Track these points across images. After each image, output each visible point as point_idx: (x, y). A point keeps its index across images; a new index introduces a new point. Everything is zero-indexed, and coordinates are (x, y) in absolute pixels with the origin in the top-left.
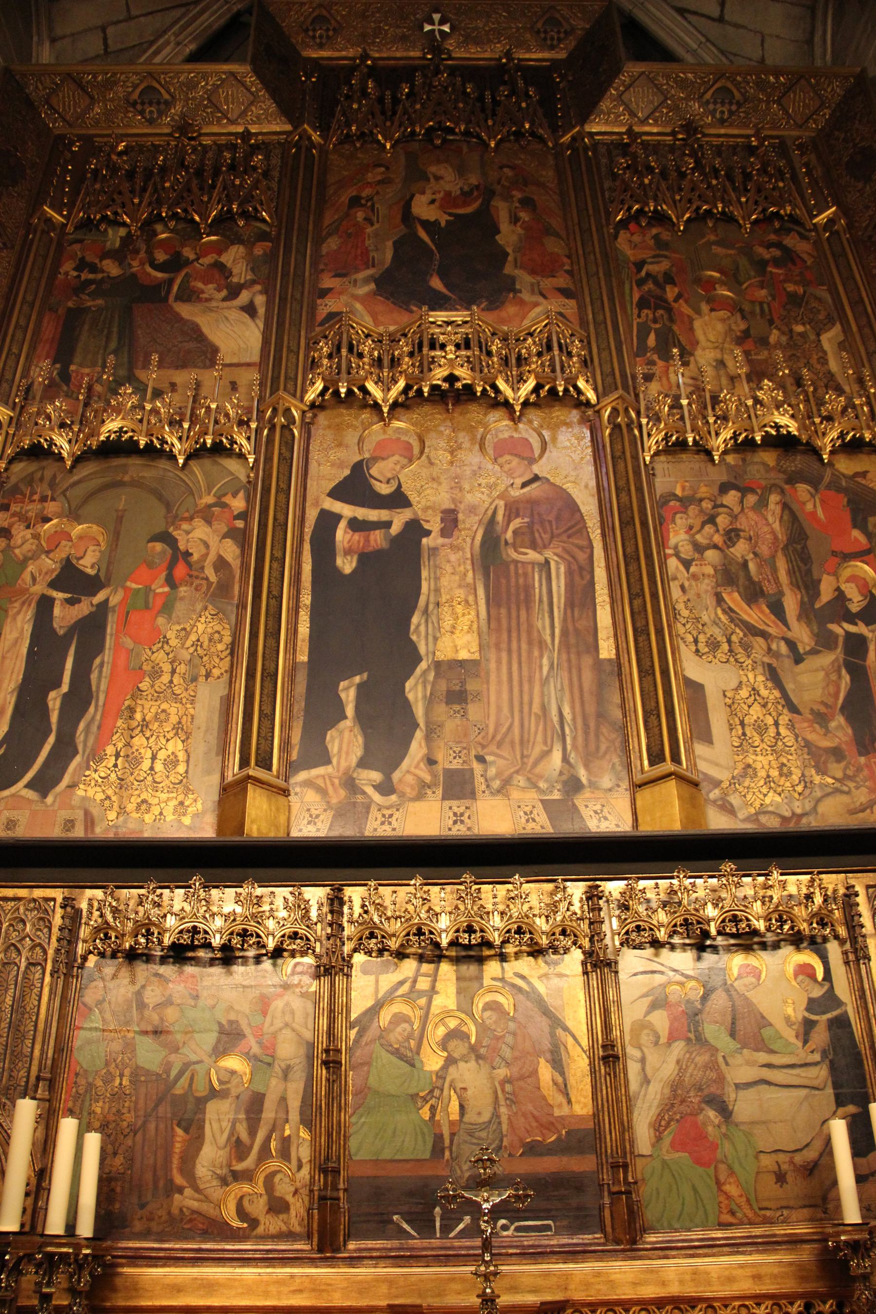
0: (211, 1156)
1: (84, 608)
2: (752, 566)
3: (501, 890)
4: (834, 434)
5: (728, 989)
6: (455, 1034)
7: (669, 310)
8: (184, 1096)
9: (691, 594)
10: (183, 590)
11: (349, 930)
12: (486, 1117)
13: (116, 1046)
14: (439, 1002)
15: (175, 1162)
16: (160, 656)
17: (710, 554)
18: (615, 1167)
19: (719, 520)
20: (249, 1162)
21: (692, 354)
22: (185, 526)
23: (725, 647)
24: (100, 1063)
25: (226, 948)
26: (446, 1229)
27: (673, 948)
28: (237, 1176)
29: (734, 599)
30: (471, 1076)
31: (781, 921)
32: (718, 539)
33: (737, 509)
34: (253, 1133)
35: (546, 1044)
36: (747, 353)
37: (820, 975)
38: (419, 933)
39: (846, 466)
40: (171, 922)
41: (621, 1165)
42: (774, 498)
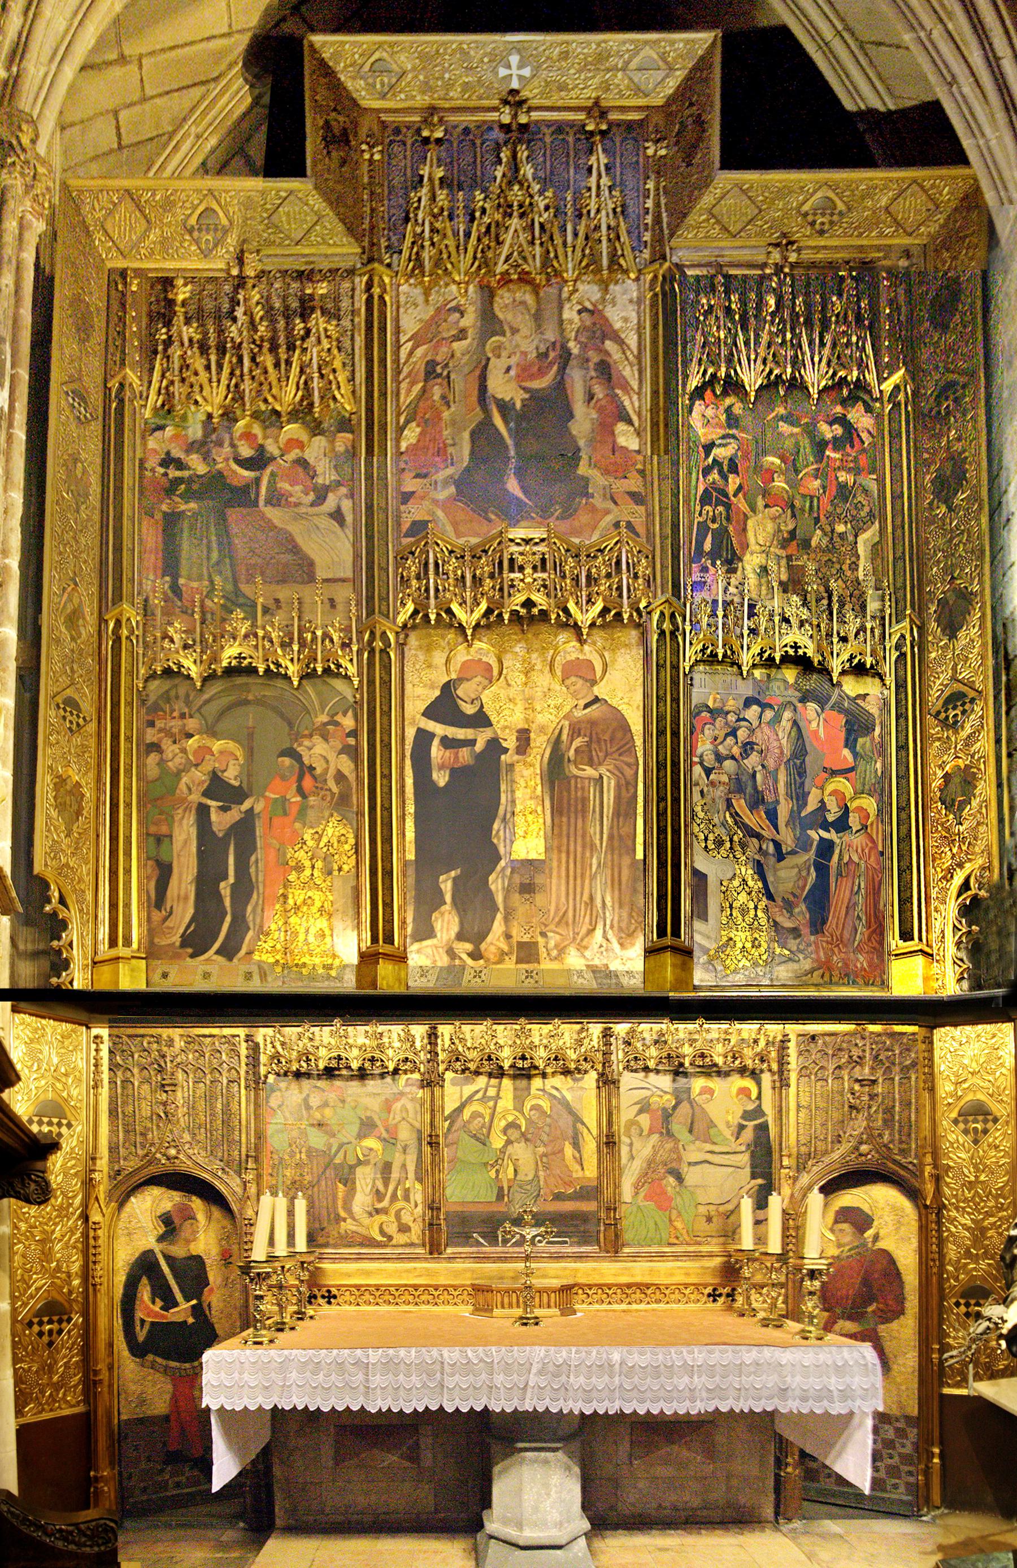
0: (361, 1200)
1: (235, 815)
2: (759, 776)
3: (546, 1029)
4: (845, 657)
5: (691, 1102)
6: (513, 1125)
7: (728, 506)
8: (341, 1165)
9: (708, 799)
10: (312, 800)
11: (442, 1056)
12: (530, 1177)
13: (295, 1133)
14: (501, 1104)
15: (340, 1203)
16: (301, 855)
17: (728, 764)
18: (608, 1209)
19: (739, 733)
20: (385, 1203)
21: (740, 560)
22: (307, 743)
23: (728, 845)
24: (286, 1145)
25: (361, 1069)
26: (505, 1241)
27: (658, 1072)
28: (378, 1211)
29: (740, 804)
30: (521, 1151)
31: (735, 1058)
32: (736, 751)
33: (755, 723)
34: (386, 1185)
35: (570, 1133)
36: (789, 558)
37: (754, 1095)
38: (490, 1059)
39: (851, 687)
40: (323, 1052)
41: (612, 1208)
42: (787, 715)
